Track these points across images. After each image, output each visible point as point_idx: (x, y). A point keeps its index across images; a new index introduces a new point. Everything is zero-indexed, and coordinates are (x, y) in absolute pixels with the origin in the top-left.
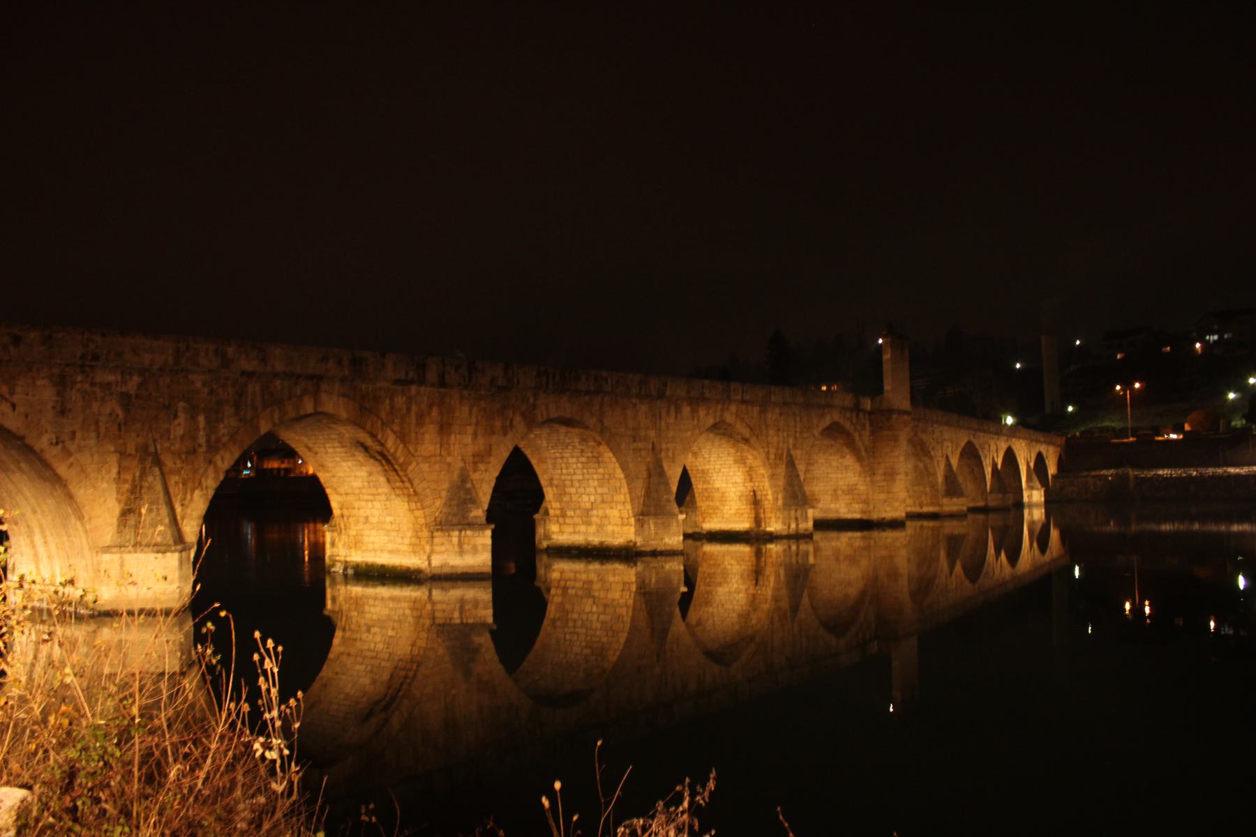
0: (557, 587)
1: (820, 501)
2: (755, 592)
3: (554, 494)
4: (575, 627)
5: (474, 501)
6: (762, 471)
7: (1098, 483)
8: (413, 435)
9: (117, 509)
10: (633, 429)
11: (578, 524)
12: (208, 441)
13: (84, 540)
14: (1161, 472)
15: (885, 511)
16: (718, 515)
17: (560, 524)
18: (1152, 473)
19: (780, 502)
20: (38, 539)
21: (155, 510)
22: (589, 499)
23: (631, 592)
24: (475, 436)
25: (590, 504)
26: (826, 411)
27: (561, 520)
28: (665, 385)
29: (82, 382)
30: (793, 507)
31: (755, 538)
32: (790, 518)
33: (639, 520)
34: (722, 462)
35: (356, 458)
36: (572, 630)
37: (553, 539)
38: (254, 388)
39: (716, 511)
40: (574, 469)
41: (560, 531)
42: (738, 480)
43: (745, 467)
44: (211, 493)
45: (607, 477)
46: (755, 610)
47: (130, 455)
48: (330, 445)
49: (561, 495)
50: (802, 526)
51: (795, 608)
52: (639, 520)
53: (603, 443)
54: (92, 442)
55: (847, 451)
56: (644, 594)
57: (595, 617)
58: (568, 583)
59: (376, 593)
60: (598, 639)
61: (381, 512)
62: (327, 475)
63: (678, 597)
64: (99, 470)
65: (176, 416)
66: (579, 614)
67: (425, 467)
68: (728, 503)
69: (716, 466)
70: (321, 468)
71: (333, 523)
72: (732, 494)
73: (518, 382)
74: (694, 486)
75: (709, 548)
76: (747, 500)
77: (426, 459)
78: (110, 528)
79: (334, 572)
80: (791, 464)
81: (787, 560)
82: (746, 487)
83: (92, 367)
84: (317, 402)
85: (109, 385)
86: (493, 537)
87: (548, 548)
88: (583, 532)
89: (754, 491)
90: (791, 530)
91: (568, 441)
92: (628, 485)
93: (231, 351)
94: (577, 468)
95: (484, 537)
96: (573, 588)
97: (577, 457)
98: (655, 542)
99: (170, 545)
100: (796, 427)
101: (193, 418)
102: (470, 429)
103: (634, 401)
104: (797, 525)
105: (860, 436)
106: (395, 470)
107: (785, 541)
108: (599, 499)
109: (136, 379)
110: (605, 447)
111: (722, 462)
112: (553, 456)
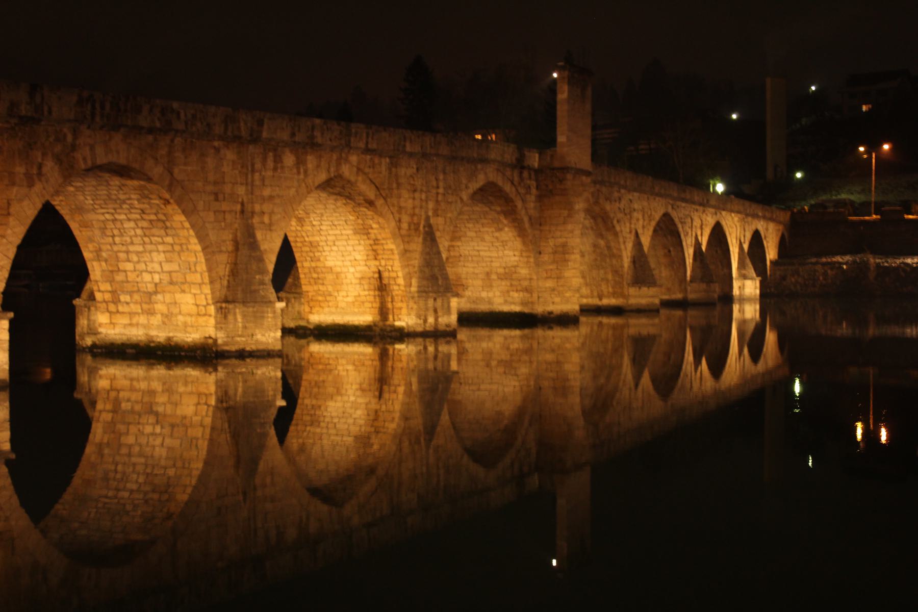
1: (467, 289)
2: (378, 407)
3: (103, 271)
4: (129, 455)
6: (391, 245)
7: (829, 272)
10: (215, 183)
11: (138, 314)
14: (909, 261)
15: (553, 303)
16: (330, 304)
17: (111, 313)
18: (898, 261)
22: (153, 279)
23: (209, 406)
25: (153, 285)
26: (479, 166)
27: (112, 307)
28: (260, 123)
30: (431, 294)
32: (427, 309)
33: (221, 308)
34: (338, 232)
37: (99, 333)
39: (328, 298)
40: (131, 237)
41: (111, 323)
42: (358, 257)
43: (368, 239)
45: (177, 248)
46: (377, 432)
49: (112, 272)
52: (221, 308)
53: (171, 201)
55: (505, 222)
56: (227, 409)
57: (158, 441)
58: (122, 394)
63: (273, 413)
68: (345, 287)
69: (330, 238)
72: (350, 276)
73: (50, 112)
74: (299, 264)
75: (317, 348)
80: (430, 237)
86: (12, 330)
87: (94, 346)
88: (142, 325)
89: (379, 272)
90: (428, 325)
91: (122, 197)
92: (207, 260)
94: (136, 236)
96: (129, 400)
97: (135, 221)
98: (243, 339)
100: (438, 187)
103: (216, 144)
104: (436, 319)
105: (524, 201)
107: (420, 340)
108: (166, 278)
110: (176, 207)
111: (338, 232)
112: (102, 218)
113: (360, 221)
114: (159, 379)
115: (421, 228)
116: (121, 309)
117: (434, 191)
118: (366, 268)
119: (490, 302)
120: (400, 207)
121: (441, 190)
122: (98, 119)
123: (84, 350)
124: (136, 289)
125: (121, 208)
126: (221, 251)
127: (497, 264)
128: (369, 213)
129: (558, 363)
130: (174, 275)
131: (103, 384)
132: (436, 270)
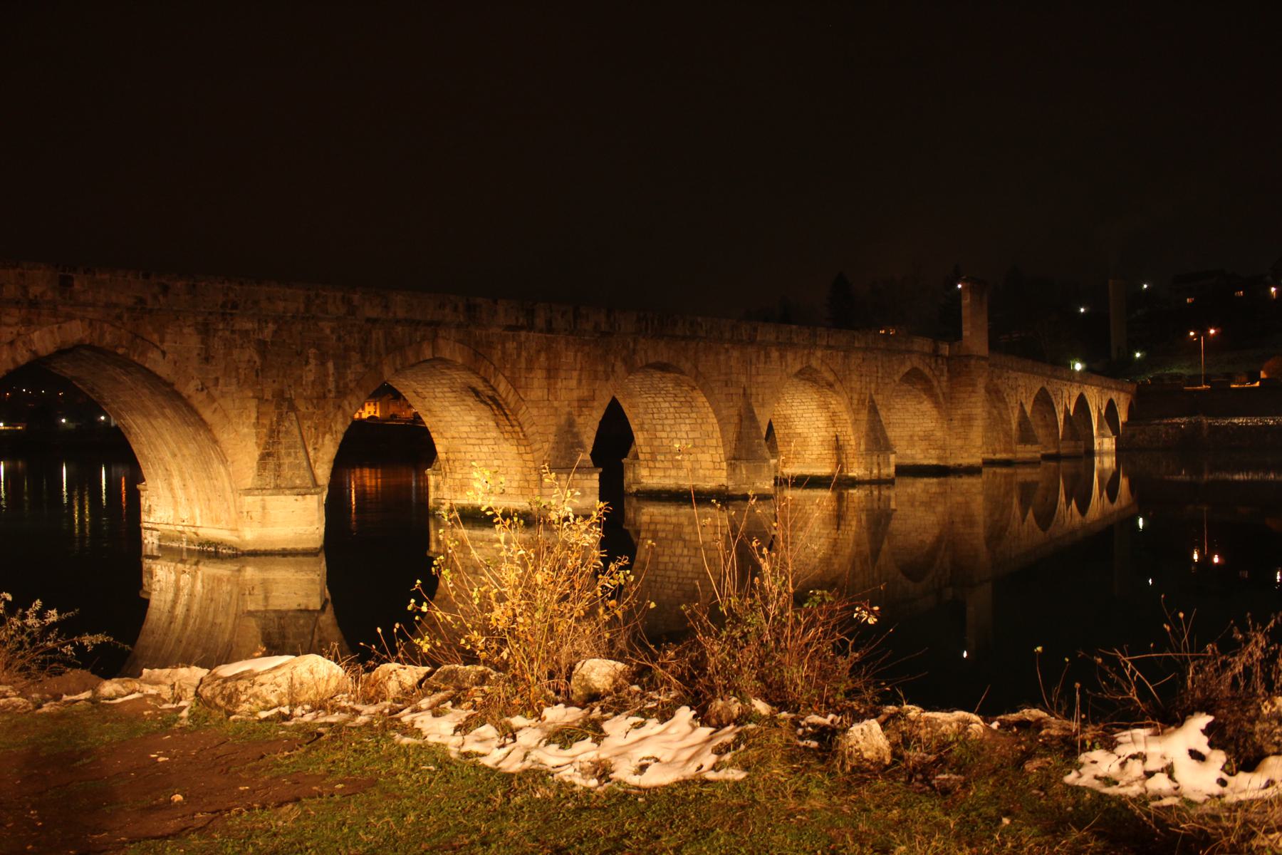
0: (648, 530)
2: (836, 536)
3: (645, 438)
4: (666, 570)
5: (581, 445)
6: (845, 416)
7: (1170, 431)
8: (523, 380)
9: (256, 454)
10: (726, 374)
11: (670, 469)
12: (337, 387)
13: (227, 485)
19: (863, 447)
20: (176, 482)
21: (293, 454)
24: (580, 381)
26: (906, 356)
27: (651, 464)
28: (755, 330)
29: (223, 329)
31: (839, 484)
33: (731, 464)
35: (465, 403)
36: (663, 572)
38: (378, 334)
40: (666, 414)
42: (820, 426)
44: (340, 437)
45: (699, 421)
46: (836, 555)
47: (267, 400)
48: (440, 390)
49: (651, 439)
50: (885, 471)
51: (876, 553)
52: (731, 464)
54: (233, 388)
55: (925, 397)
57: (686, 560)
58: (658, 527)
59: (483, 535)
60: (690, 581)
61: (488, 455)
62: (433, 419)
64: (240, 415)
65: (307, 363)
66: (670, 557)
67: (534, 412)
68: (810, 448)
69: (799, 411)
70: (427, 413)
71: (437, 468)
72: (814, 439)
73: (619, 325)
74: (776, 432)
76: (829, 445)
77: (536, 403)
78: (251, 471)
79: (439, 515)
80: (873, 410)
81: (869, 506)
82: (829, 432)
83: (231, 314)
84: (435, 348)
85: (247, 332)
86: (601, 480)
87: (638, 491)
89: (837, 436)
91: (662, 385)
92: (721, 430)
93: (356, 298)
94: (670, 413)
95: (591, 480)
96: (663, 531)
97: (669, 402)
99: (308, 488)
100: (877, 372)
101: (323, 364)
102: (575, 374)
103: (726, 346)
104: (879, 470)
105: (939, 382)
106: (506, 415)
107: (868, 486)
109: (271, 326)
112: (646, 401)
113: (822, 399)
114: (686, 515)
115: (867, 403)
116: (657, 465)
117: (875, 375)
118: (826, 434)
119: (913, 458)
120: (851, 388)
121: (880, 375)
122: (649, 331)
123: (630, 494)
124: (668, 451)
125: (660, 393)
126: (730, 423)
127: (919, 429)
128: (831, 393)
129: (967, 503)
130: (697, 440)
131: (645, 518)
132: (879, 434)
